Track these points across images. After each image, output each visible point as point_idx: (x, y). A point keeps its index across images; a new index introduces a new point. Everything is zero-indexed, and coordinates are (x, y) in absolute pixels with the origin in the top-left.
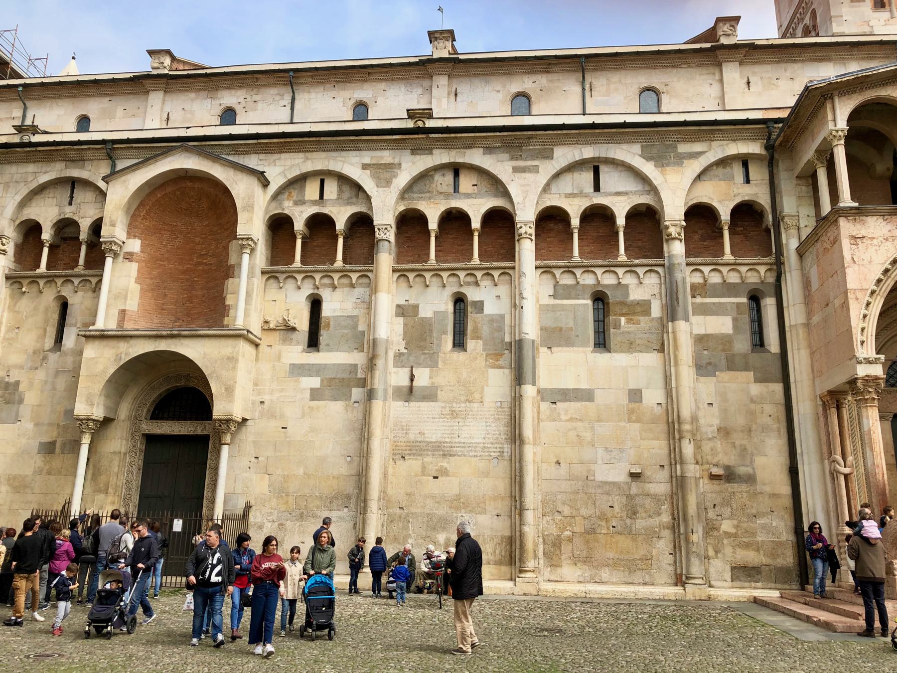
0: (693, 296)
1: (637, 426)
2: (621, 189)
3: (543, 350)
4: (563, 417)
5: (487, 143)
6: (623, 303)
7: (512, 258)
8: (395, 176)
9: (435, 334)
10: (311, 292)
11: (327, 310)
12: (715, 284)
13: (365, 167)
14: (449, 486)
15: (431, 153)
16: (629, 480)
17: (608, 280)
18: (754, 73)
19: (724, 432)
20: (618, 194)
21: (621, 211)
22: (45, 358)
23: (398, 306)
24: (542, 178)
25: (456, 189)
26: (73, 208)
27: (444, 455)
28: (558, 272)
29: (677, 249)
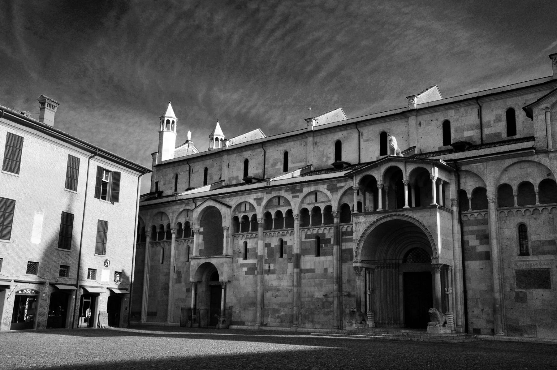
0: (342, 236)
1: (326, 280)
2: (322, 201)
3: (302, 256)
4: (307, 278)
5: (285, 189)
6: (324, 240)
7: (294, 227)
8: (262, 202)
9: (275, 253)
10: (244, 241)
11: (249, 246)
12: (349, 231)
13: (255, 199)
14: (279, 300)
15: (271, 193)
16: (323, 297)
17: (320, 232)
18: (423, 119)
19: (349, 281)
20: (322, 202)
21: (322, 207)
22: (186, 264)
23: (266, 244)
24: (299, 200)
25: (279, 205)
26: (188, 218)
27: (277, 291)
28: (306, 230)
29: (336, 220)
